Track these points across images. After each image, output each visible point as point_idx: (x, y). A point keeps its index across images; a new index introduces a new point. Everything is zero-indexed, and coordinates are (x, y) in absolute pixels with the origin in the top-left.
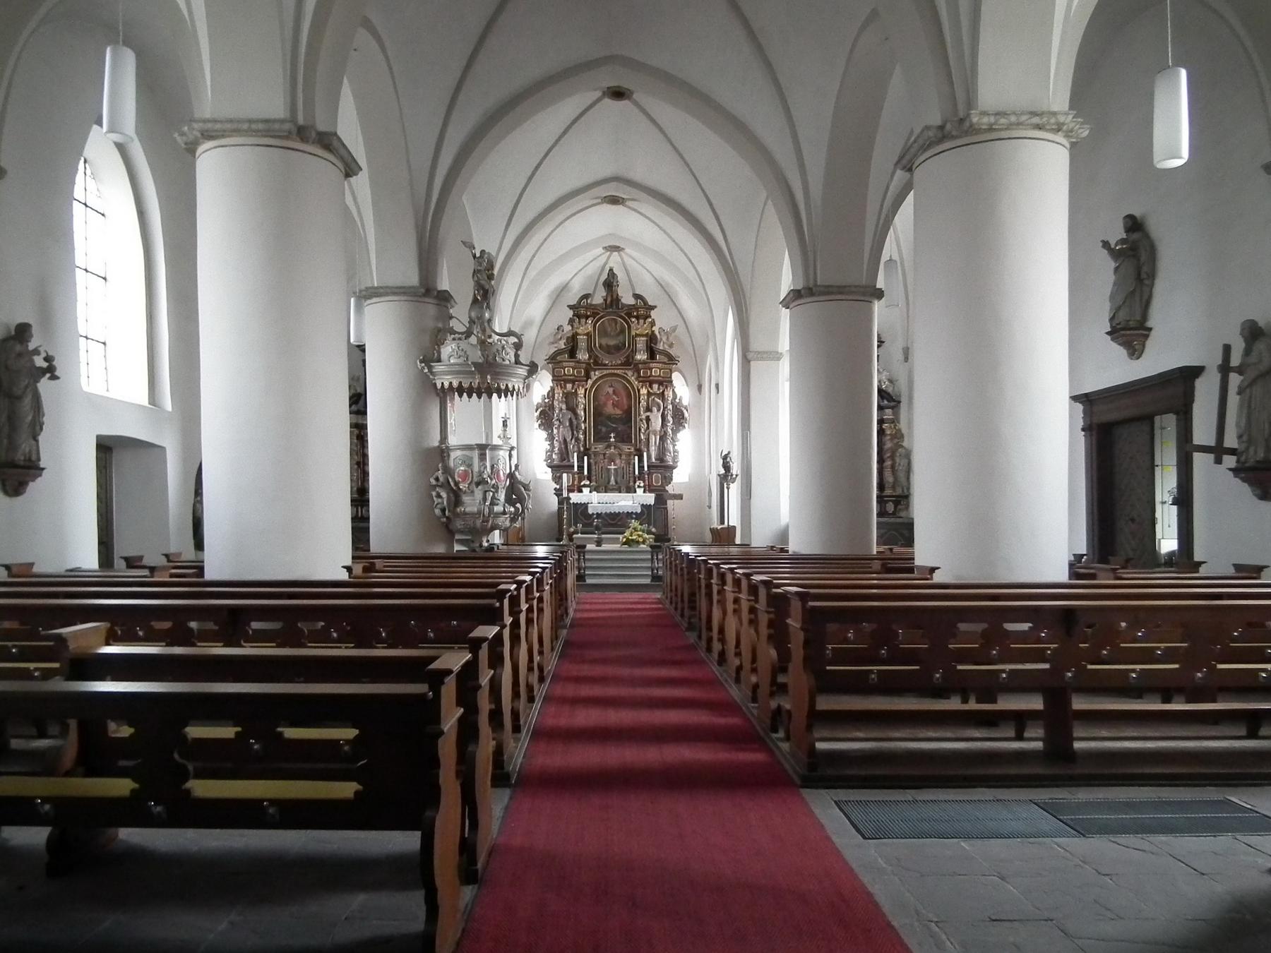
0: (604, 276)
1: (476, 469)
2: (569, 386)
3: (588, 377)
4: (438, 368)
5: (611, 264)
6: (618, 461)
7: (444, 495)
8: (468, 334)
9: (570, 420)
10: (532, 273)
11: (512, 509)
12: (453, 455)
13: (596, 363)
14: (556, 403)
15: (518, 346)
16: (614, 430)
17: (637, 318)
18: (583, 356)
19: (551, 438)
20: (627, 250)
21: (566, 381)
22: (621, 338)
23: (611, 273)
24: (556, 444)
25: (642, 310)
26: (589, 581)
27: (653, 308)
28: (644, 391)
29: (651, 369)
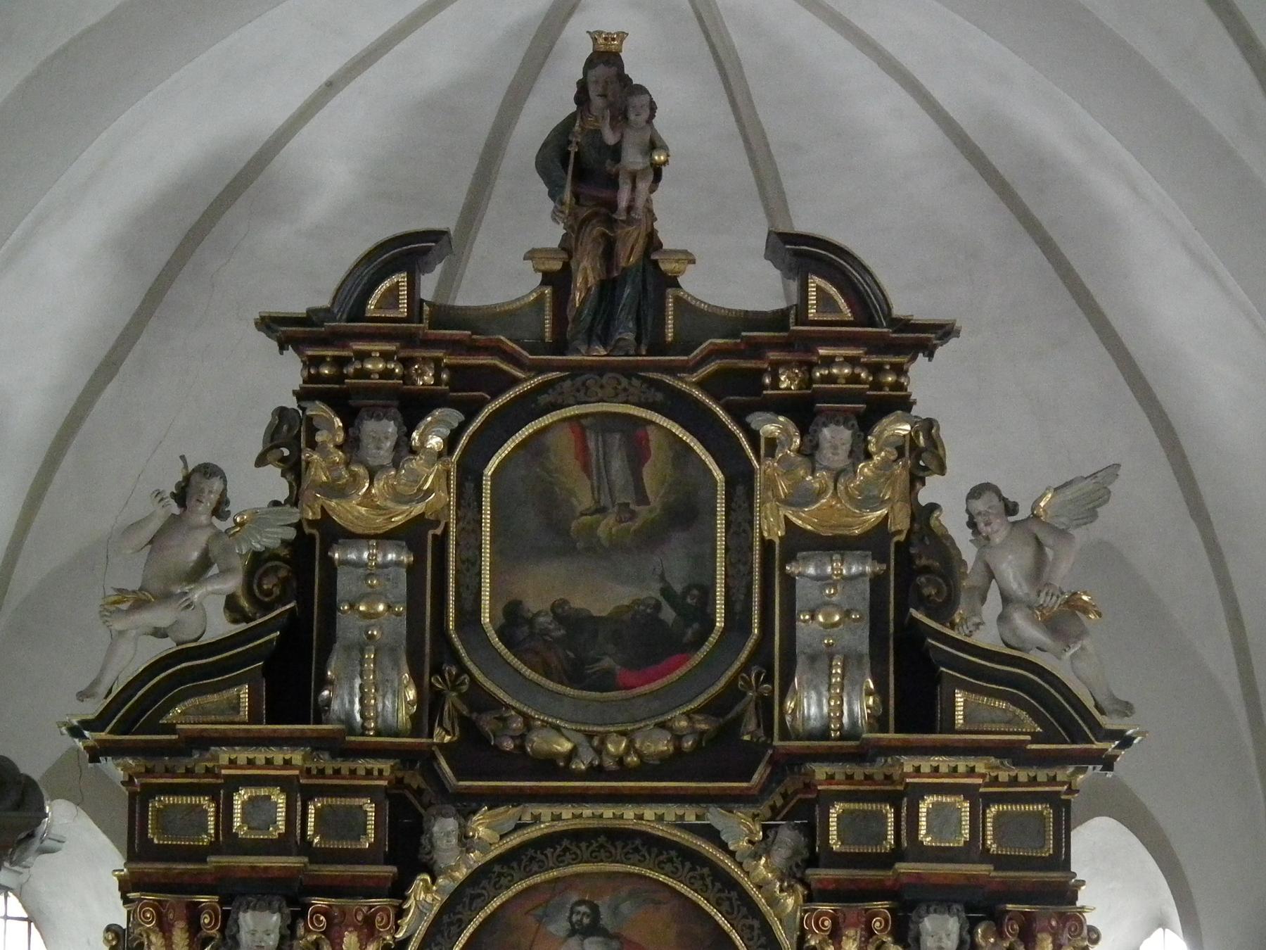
0: (552, 102)
3: (408, 854)
13: (475, 751)
17: (804, 412)
18: (372, 695)
21: (238, 892)
22: (674, 563)
23: (609, 85)
25: (842, 347)
27: (924, 338)
29: (904, 797)
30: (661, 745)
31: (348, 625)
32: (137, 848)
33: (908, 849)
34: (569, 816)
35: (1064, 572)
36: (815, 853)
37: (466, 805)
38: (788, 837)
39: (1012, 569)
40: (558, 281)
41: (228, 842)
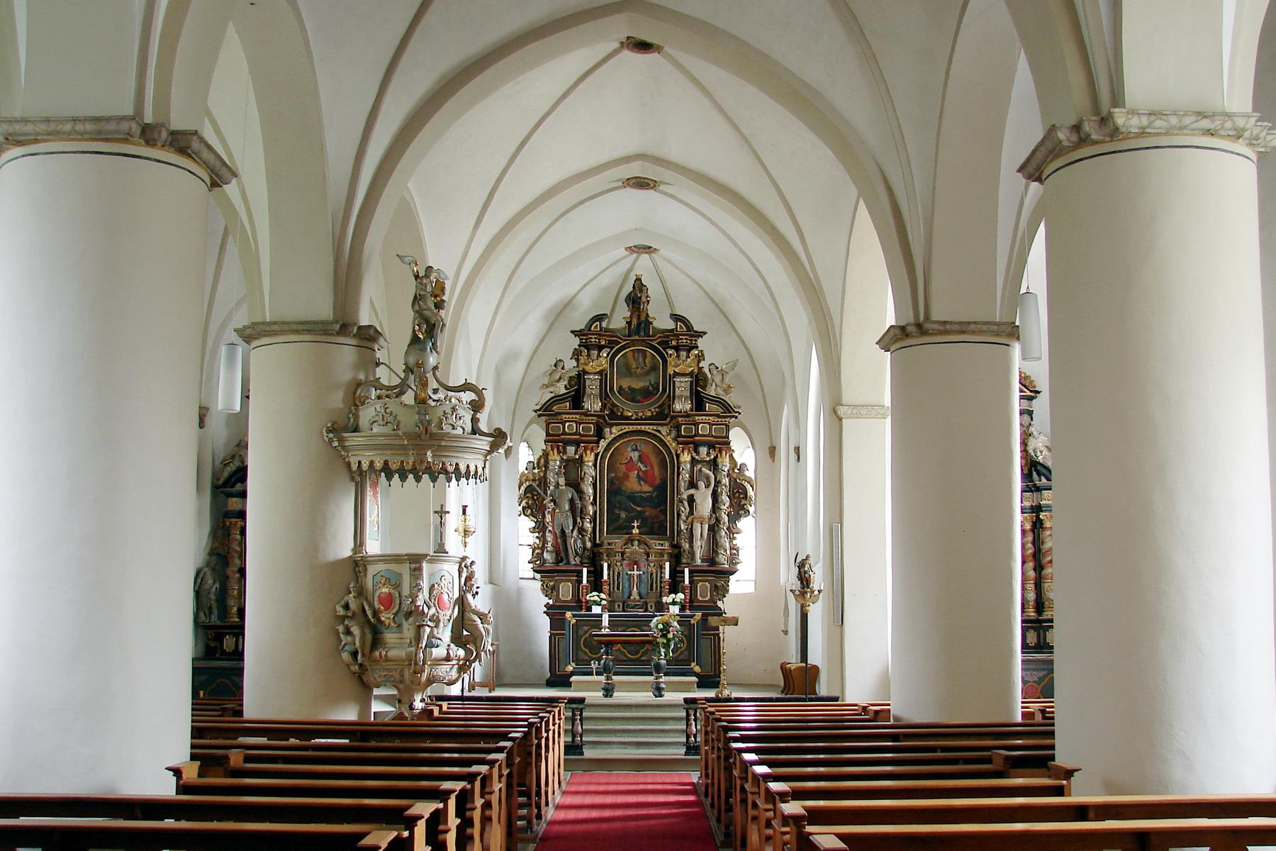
0: (628, 288)
1: (406, 591)
2: (571, 450)
3: (600, 435)
4: (353, 440)
5: (638, 271)
6: (643, 563)
7: (356, 630)
8: (401, 389)
9: (572, 501)
10: (519, 285)
11: (461, 653)
12: (372, 570)
13: (613, 415)
14: (551, 478)
15: (477, 406)
16: (639, 516)
17: (677, 349)
18: (593, 404)
19: (540, 528)
20: (664, 252)
21: (567, 443)
22: (652, 378)
23: (639, 285)
24: (549, 537)
25: (684, 336)
26: (589, 753)
28: (686, 457)
29: (696, 424)
30: (649, 414)
31: (588, 391)
32: (548, 434)
33: (697, 434)
34: (631, 428)
35: (727, 380)
36: (679, 435)
37: (611, 426)
38: (674, 433)
39: (718, 379)
40: (629, 323)
41: (564, 433)
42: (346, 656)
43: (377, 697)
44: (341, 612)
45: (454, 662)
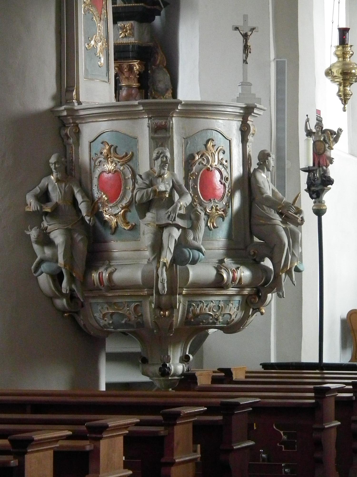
7: (58, 237)
11: (245, 274)
12: (89, 131)
42: (44, 281)
43: (113, 358)
44: (32, 204)
45: (231, 291)
